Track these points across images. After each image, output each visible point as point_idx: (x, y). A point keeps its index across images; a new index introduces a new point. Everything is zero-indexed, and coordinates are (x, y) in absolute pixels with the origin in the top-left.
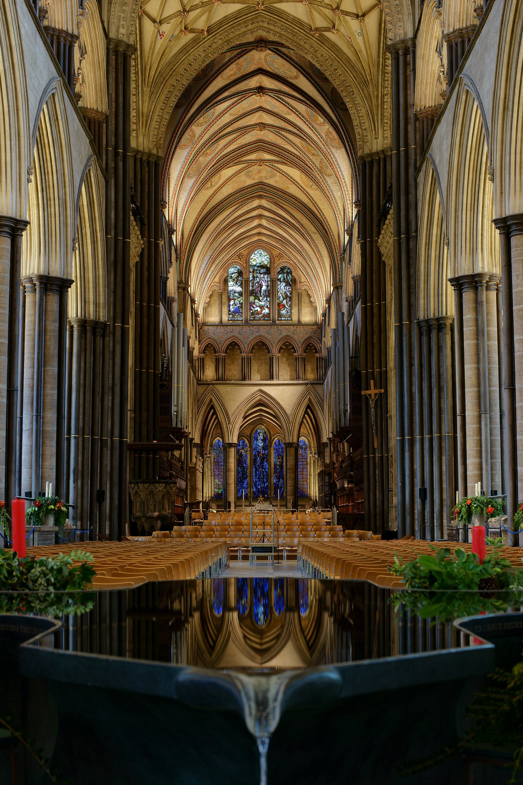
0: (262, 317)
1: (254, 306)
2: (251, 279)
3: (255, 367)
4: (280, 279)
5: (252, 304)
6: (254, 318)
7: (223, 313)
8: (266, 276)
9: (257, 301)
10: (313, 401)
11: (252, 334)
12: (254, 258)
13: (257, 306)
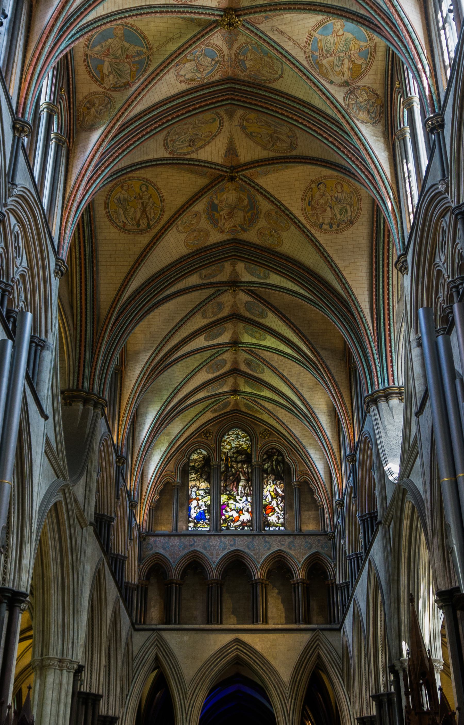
0: (239, 526)
1: (228, 509)
2: (223, 470)
3: (228, 605)
4: (267, 469)
5: (223, 507)
6: (222, 460)
7: (180, 519)
8: (245, 466)
9: (231, 501)
10: (325, 659)
11: (224, 549)
12: (228, 440)
13: (232, 510)
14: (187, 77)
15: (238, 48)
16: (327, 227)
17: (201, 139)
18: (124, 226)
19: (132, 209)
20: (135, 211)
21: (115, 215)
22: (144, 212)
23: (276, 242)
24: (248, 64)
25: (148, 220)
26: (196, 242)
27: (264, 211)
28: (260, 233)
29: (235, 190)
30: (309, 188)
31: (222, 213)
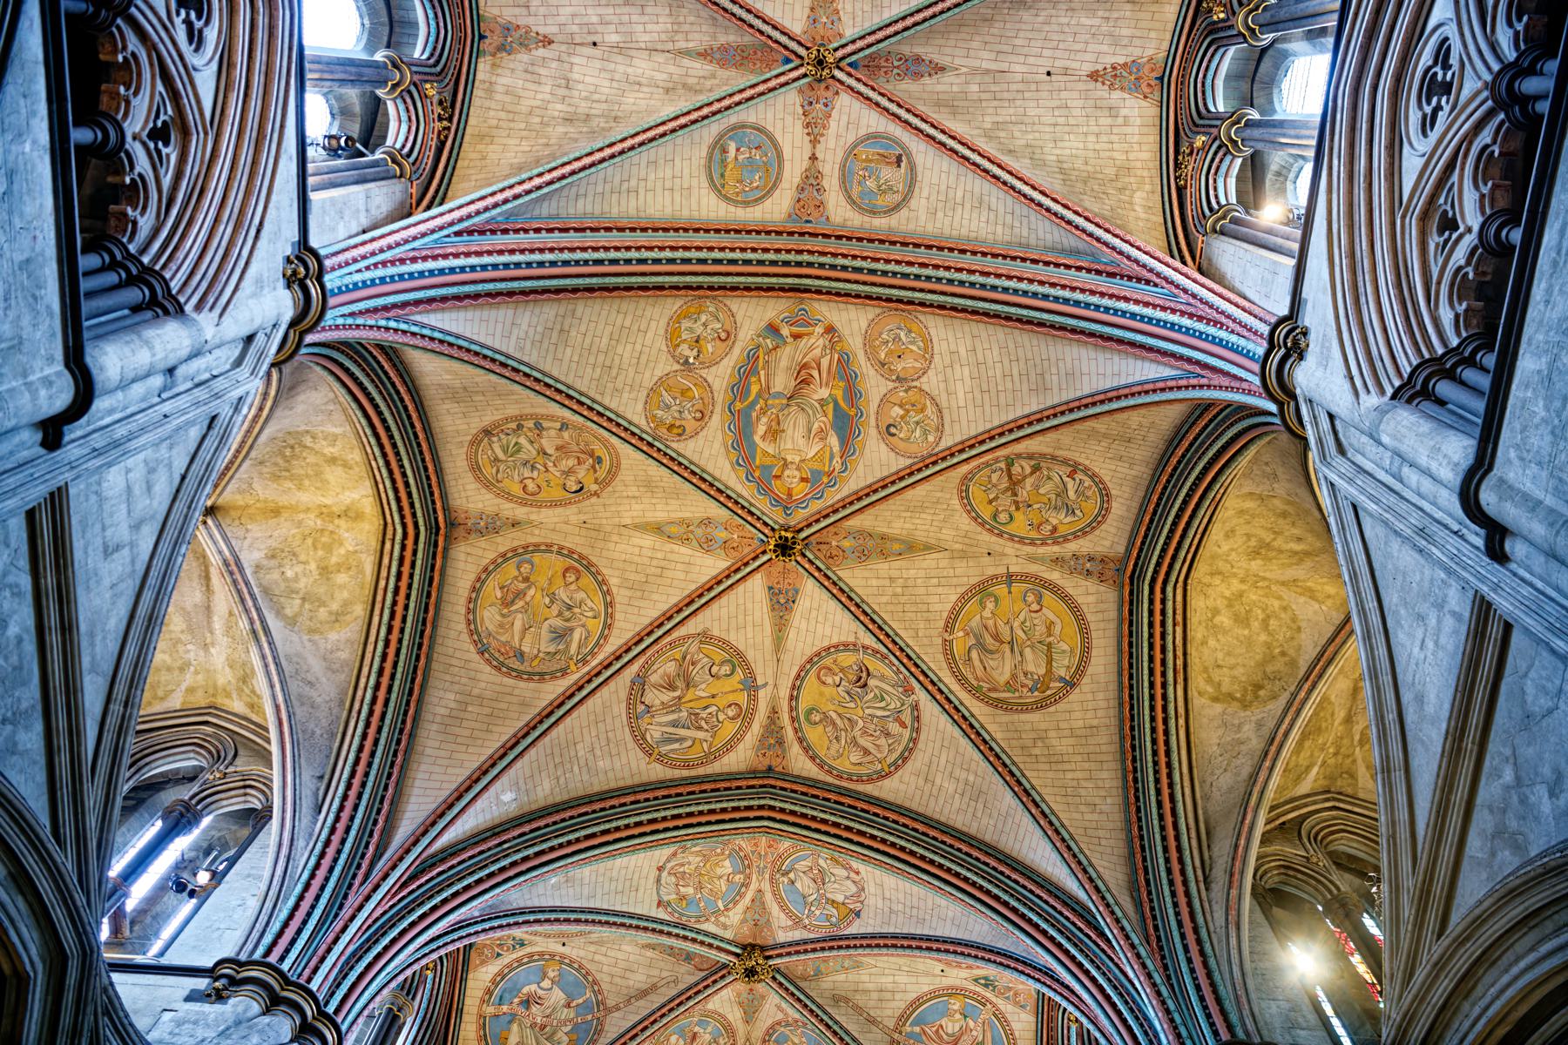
14: (844, 873)
15: (742, 896)
16: (545, 424)
17: (842, 670)
18: (1074, 472)
19: (1042, 491)
20: (1037, 488)
21: (1089, 493)
22: (1014, 484)
23: (686, 324)
24: (727, 867)
25: (1009, 470)
26: (902, 335)
27: (716, 421)
28: (727, 337)
29: (786, 465)
30: (604, 483)
31: (824, 393)
